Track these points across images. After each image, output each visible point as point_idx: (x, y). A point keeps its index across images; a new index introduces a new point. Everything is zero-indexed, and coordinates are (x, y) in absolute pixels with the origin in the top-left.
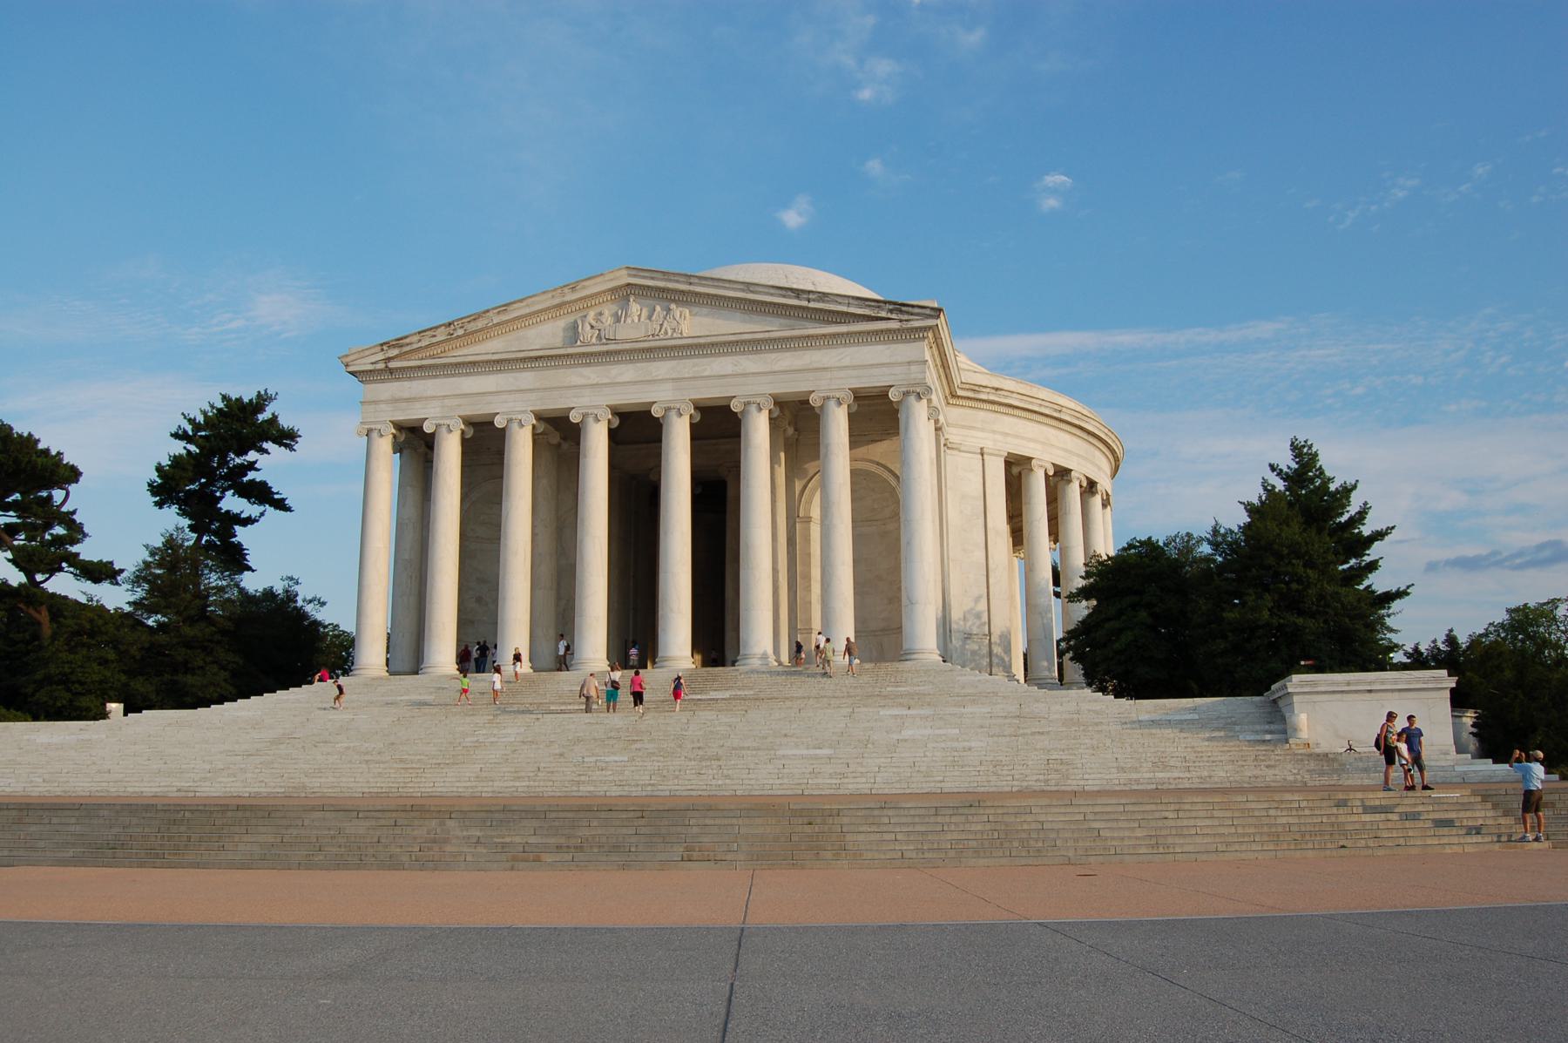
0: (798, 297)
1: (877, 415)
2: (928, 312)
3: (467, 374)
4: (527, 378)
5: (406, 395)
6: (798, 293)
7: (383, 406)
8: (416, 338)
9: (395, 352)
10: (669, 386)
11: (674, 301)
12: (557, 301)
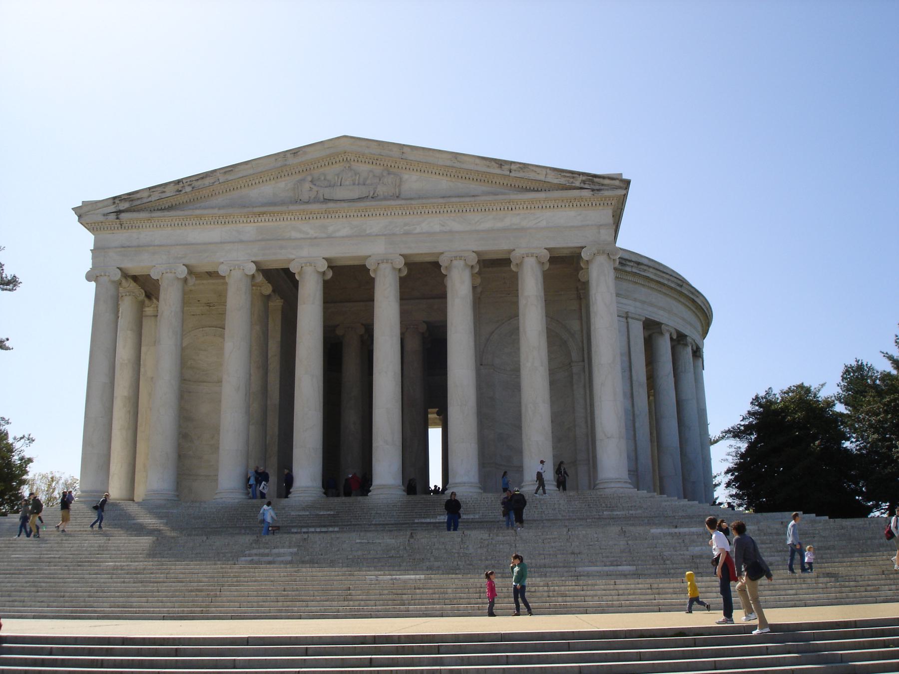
1: (566, 273)
2: (617, 183)
9: (126, 205)
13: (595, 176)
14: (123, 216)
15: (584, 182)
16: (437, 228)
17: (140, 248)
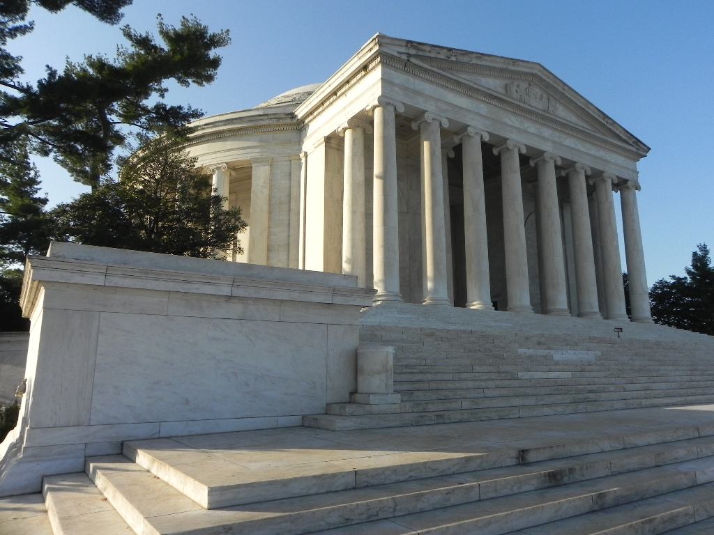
0: (604, 119)
4: (483, 108)
7: (397, 89)
8: (428, 49)
11: (551, 95)
12: (504, 66)
13: (639, 141)
14: (412, 60)
15: (634, 142)
16: (573, 145)
17: (417, 93)
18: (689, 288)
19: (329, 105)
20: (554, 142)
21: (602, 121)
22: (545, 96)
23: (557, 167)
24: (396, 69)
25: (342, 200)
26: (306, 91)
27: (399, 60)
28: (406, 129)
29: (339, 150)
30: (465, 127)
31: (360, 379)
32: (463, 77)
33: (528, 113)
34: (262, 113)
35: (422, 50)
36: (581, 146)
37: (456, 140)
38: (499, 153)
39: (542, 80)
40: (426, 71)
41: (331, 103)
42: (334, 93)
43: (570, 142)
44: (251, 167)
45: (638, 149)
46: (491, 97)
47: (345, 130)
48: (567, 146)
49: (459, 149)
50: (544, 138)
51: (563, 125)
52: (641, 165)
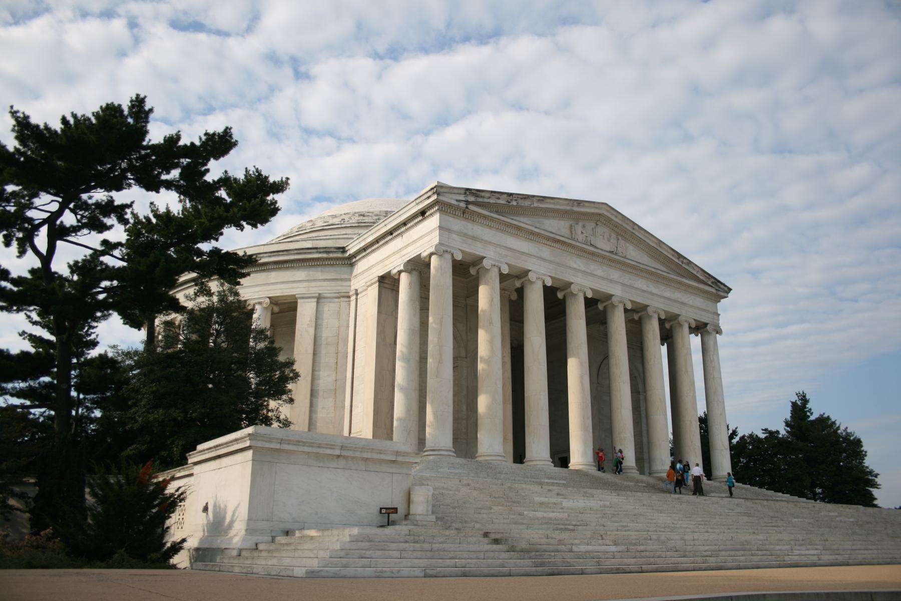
3: (512, 234)
4: (546, 252)
5: (470, 233)
6: (680, 256)
7: (454, 236)
8: (488, 195)
10: (619, 287)
12: (568, 208)
14: (471, 207)
16: (645, 288)
17: (474, 238)
18: (782, 442)
19: (383, 244)
20: (624, 285)
21: (676, 260)
22: (613, 235)
23: (626, 311)
24: (455, 216)
25: (395, 343)
26: (357, 211)
27: (457, 208)
28: (466, 274)
29: (393, 290)
30: (527, 272)
31: (411, 506)
32: (524, 222)
33: (593, 255)
34: (310, 246)
35: (481, 197)
36: (653, 288)
37: (518, 284)
38: (564, 296)
39: (610, 220)
40: (485, 217)
41: (387, 242)
42: (390, 232)
43: (641, 284)
44: (296, 302)
45: (717, 289)
46: (554, 241)
47: (400, 272)
48: (637, 289)
49: (520, 292)
50: (611, 281)
51: (632, 266)
52: (723, 305)
